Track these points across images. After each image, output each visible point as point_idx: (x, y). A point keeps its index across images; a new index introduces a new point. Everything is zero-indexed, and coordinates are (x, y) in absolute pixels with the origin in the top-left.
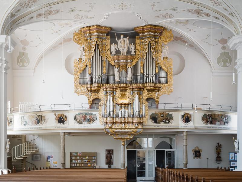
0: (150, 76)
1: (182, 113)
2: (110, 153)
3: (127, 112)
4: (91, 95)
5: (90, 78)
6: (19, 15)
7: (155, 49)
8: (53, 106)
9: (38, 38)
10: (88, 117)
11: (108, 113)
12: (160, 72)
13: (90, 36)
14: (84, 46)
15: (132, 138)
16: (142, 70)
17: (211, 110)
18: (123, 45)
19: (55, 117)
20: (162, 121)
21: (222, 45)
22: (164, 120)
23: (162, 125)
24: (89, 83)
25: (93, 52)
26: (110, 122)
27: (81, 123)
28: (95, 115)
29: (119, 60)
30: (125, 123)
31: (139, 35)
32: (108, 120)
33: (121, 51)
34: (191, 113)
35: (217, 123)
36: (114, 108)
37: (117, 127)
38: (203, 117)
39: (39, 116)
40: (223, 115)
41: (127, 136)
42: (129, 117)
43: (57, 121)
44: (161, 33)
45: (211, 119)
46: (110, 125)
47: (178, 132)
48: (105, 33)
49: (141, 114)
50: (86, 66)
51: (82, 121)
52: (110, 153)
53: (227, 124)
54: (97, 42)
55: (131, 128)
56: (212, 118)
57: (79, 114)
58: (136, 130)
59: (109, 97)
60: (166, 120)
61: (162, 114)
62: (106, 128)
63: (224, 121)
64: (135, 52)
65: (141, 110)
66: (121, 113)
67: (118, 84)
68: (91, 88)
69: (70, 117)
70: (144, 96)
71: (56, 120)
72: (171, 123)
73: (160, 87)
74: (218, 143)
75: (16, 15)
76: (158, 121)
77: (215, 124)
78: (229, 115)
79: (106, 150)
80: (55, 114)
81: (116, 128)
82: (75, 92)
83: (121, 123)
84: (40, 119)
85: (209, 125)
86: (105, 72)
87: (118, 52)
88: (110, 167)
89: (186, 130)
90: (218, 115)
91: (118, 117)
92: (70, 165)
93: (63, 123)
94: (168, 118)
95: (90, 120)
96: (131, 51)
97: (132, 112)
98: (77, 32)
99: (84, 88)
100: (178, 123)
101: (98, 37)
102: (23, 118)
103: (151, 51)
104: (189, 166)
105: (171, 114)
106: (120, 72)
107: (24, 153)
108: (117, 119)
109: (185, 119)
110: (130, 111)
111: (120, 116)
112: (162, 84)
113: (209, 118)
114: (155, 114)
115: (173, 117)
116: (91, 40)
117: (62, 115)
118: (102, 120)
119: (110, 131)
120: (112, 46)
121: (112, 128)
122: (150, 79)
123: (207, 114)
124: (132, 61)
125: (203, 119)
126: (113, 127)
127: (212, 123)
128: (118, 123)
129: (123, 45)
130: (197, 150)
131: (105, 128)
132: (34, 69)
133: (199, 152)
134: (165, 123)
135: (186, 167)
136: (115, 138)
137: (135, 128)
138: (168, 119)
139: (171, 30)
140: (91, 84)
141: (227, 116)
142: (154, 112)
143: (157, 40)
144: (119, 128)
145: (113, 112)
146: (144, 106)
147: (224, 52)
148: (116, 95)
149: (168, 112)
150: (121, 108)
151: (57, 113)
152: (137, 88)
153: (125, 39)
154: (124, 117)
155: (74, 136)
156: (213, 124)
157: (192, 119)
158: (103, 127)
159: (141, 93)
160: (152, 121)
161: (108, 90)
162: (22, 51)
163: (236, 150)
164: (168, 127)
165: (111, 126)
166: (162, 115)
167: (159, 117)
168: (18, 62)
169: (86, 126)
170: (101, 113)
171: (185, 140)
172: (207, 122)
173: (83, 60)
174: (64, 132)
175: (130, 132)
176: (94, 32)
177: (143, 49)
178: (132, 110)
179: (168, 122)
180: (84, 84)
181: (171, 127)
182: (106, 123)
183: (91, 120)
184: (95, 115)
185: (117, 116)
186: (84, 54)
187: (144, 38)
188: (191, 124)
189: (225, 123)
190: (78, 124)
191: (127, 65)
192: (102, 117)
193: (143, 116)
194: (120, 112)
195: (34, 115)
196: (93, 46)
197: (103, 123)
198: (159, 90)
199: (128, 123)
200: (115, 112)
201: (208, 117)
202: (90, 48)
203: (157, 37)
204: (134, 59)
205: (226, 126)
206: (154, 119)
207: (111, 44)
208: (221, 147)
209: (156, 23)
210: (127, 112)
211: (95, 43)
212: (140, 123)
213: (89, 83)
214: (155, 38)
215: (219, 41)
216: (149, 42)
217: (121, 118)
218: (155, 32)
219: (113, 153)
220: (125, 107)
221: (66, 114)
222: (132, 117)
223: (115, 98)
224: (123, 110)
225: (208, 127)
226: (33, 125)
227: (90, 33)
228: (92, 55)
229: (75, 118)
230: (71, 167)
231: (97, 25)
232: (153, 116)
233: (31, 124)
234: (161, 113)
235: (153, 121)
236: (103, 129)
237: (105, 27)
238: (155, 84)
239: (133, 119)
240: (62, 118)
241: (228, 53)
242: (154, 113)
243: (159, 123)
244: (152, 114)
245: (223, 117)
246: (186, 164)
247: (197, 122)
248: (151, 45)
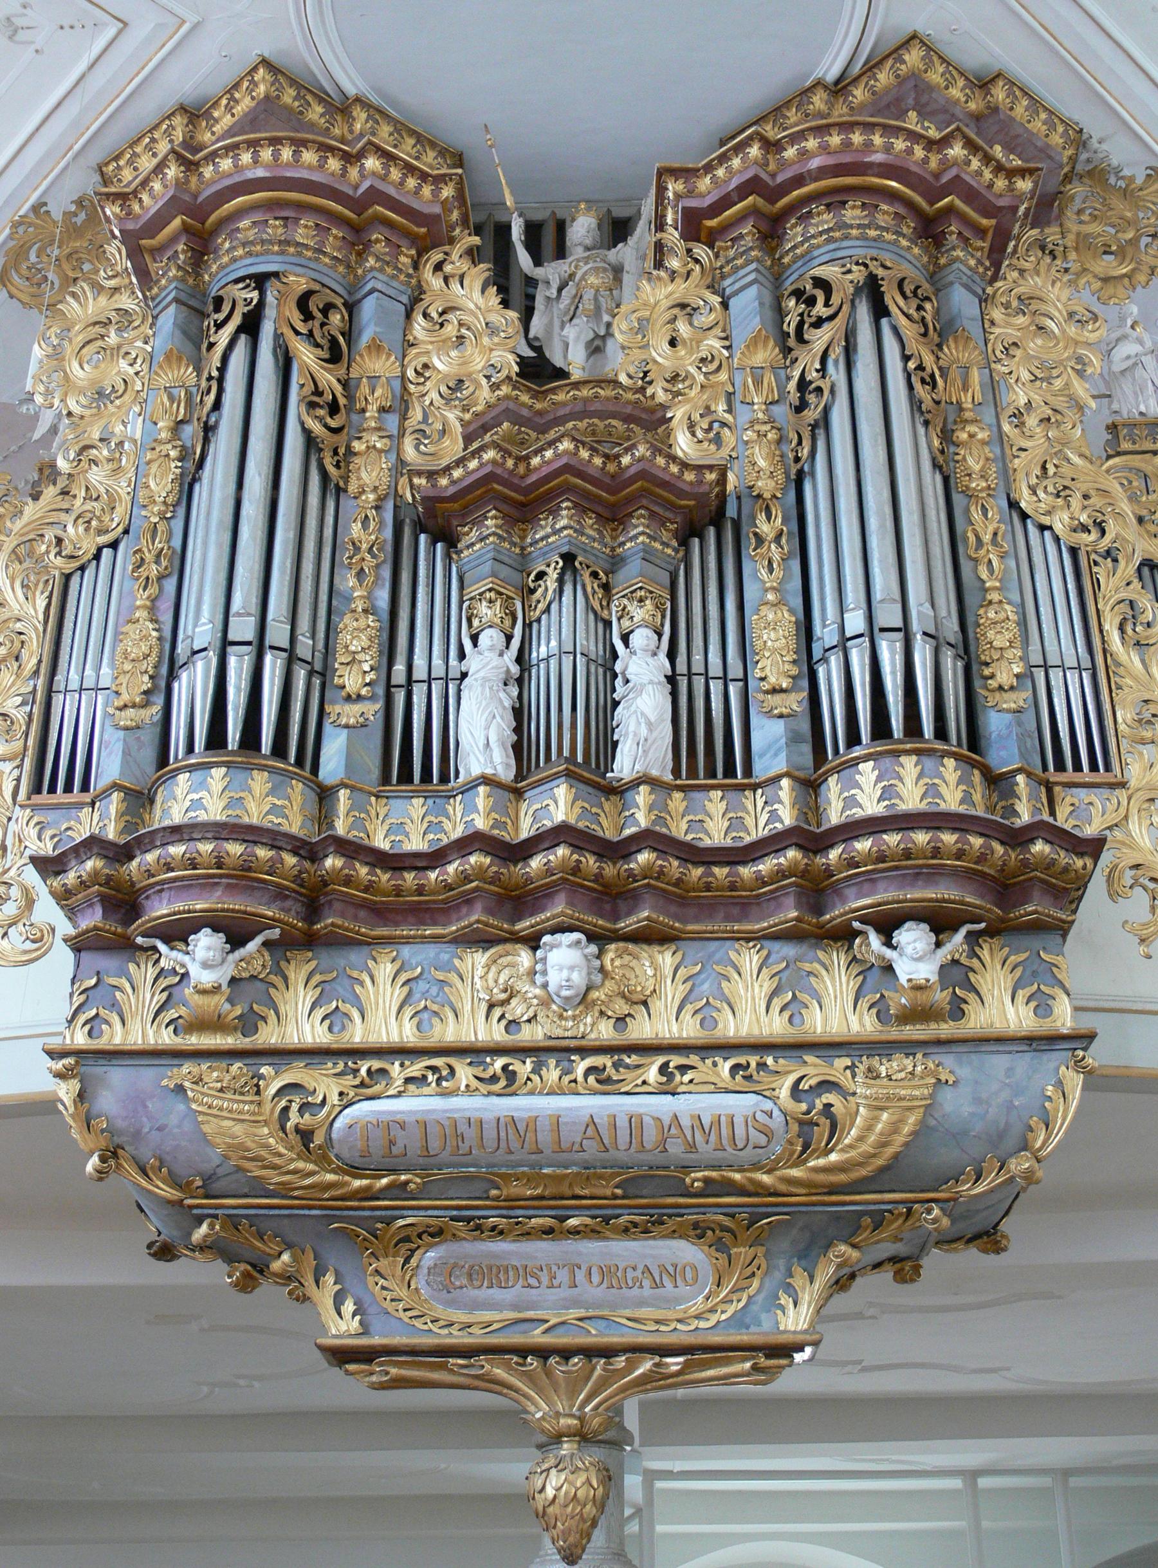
3: (643, 667)
11: (193, 687)
26: (198, 876)
32: (177, 816)
42: (708, 754)
55: (776, 1026)
62: (116, 1036)
81: (357, 1035)
83: (504, 900)
111: (481, 737)
119: (220, 1118)
121: (268, 1036)
126: (299, 1021)
128: (424, 910)
131: (80, 1039)
136: (343, 1327)
137: (862, 1024)
144: (449, 1032)
145: (323, 673)
154: (594, 772)
165: (251, 996)
182: (117, 916)
185: (412, 761)
194: (488, 661)
197: (47, 911)
210: (643, 667)
223: (374, 399)
224: (563, 629)
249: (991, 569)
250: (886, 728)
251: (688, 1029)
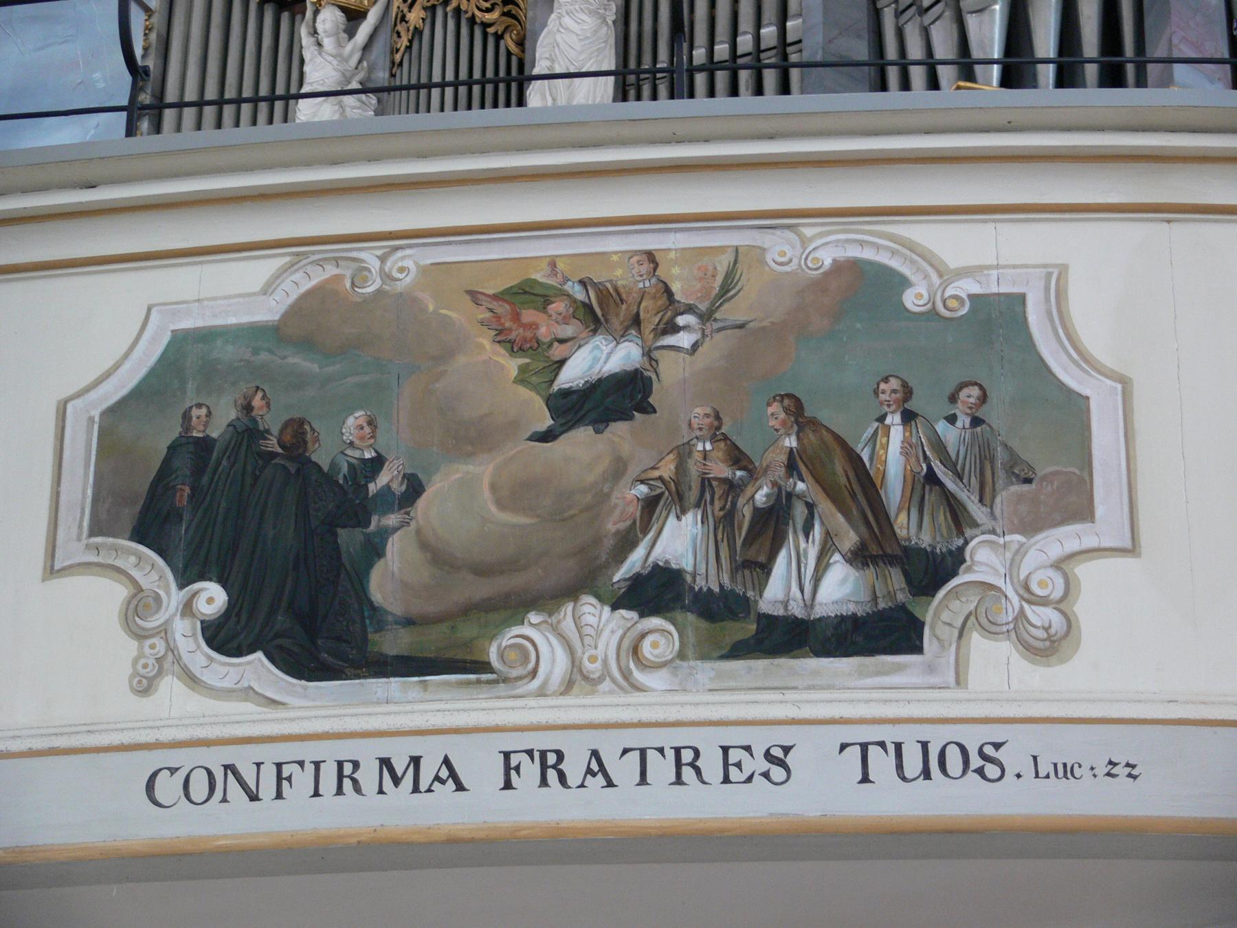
22: (680, 541)
23: (593, 721)
60: (771, 525)
61: (600, 312)
76: (394, 577)
105: (999, 318)
115: (1072, 412)
138: (860, 493)
142: (240, 293)
149: (828, 249)
160: (138, 607)
167: (472, 438)
179: (839, 589)
181: (985, 762)
232: (219, 419)
234: (529, 294)
235: (212, 598)
242: (269, 311)
244: (187, 360)
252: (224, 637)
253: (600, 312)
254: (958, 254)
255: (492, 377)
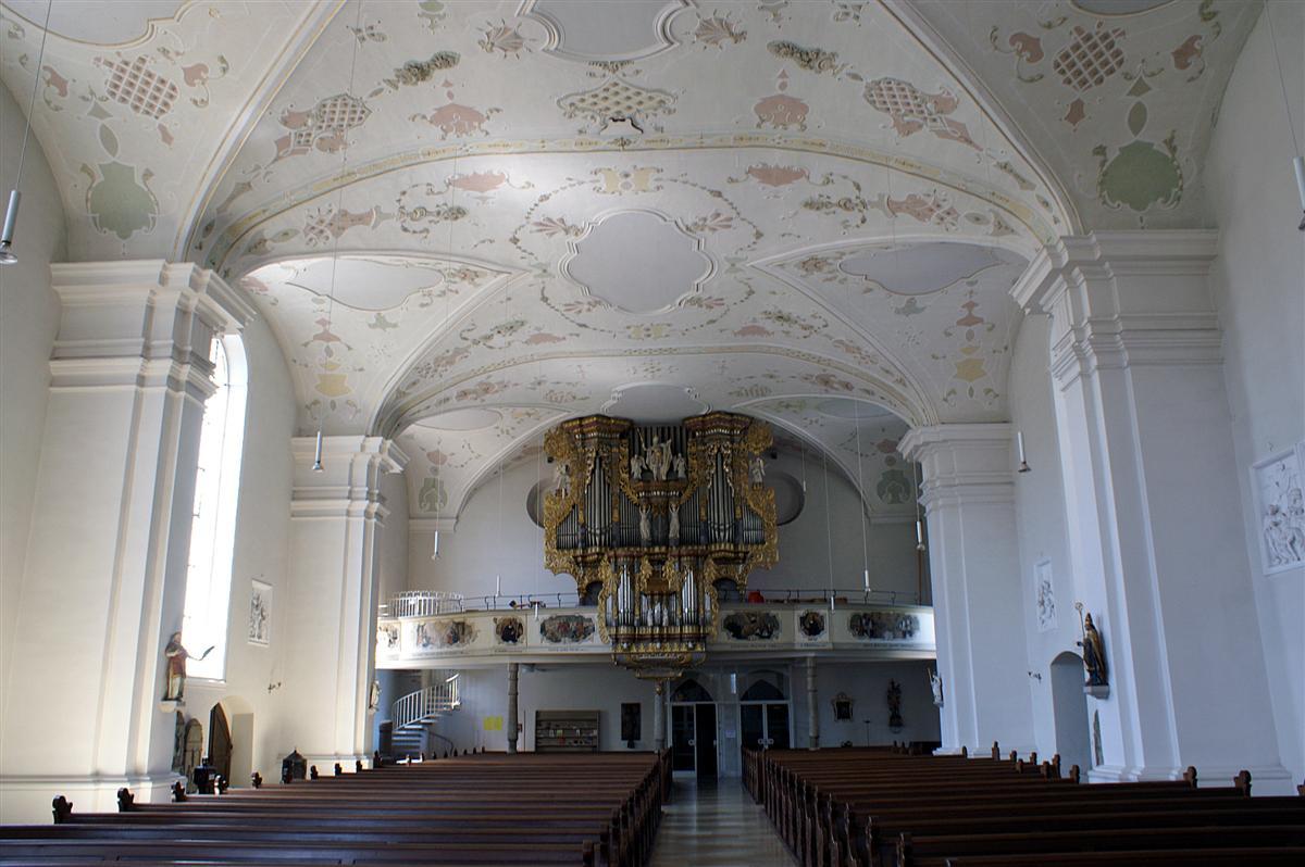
0: (722, 527)
1: (801, 612)
2: (631, 714)
3: (665, 613)
4: (584, 575)
5: (582, 534)
6: (414, 393)
7: (731, 466)
8: (491, 601)
9: (466, 446)
10: (573, 626)
12: (745, 519)
13: (583, 440)
14: (568, 462)
15: (680, 675)
16: (703, 513)
17: (870, 605)
18: (658, 460)
19: (493, 626)
20: (752, 632)
21: (885, 455)
22: (758, 631)
23: (753, 644)
24: (580, 545)
25: (588, 474)
27: (558, 641)
28: (590, 620)
29: (649, 492)
30: (661, 639)
31: (694, 436)
33: (655, 472)
34: (823, 612)
35: (887, 634)
36: (635, 601)
37: (642, 650)
38: (852, 621)
39: (458, 624)
40: (898, 615)
41: (668, 671)
42: (671, 623)
43: (500, 637)
44: (745, 430)
45: (870, 625)
46: (625, 645)
47: (793, 659)
48: (617, 432)
49: (701, 616)
50: (573, 507)
51: (558, 635)
52: (631, 714)
53: (911, 635)
54: (597, 453)
56: (873, 624)
57: (551, 619)
58: (689, 655)
59: (624, 577)
61: (753, 615)
63: (904, 628)
64: (686, 472)
65: (701, 606)
66: (653, 612)
67: (649, 548)
68: (583, 557)
69: (532, 623)
70: (706, 574)
71: (497, 633)
72: (774, 639)
73: (747, 553)
74: (893, 683)
75: (409, 394)
77: (881, 637)
78: (912, 614)
79: (623, 705)
80: (495, 620)
82: (548, 566)
83: (653, 639)
84: (458, 633)
85: (866, 640)
86: (615, 520)
87: (646, 471)
88: (631, 745)
89: (813, 655)
90: (889, 614)
91: (646, 625)
92: (536, 742)
93: (515, 641)
94: (768, 627)
95: (578, 634)
96: (677, 471)
97: (678, 613)
98: (553, 431)
99: (564, 559)
100: (791, 635)
101: (601, 441)
102: (420, 628)
103: (723, 470)
104: (824, 743)
106: (651, 521)
107: (423, 714)
108: (643, 631)
109: (808, 626)
110: (673, 609)
111: (650, 623)
112: (752, 544)
113: (867, 624)
114: (736, 615)
116: (584, 448)
117: (512, 621)
118: (607, 634)
119: (626, 658)
120: (633, 462)
122: (722, 534)
123: (861, 612)
124: (680, 494)
125: (852, 627)
127: (873, 635)
129: (658, 460)
130: (843, 700)
132: (457, 518)
133: (847, 704)
134: (762, 637)
135: (817, 745)
139: (767, 422)
140: (585, 548)
141: (909, 617)
142: (732, 612)
143: (736, 445)
146: (707, 597)
147: (893, 471)
148: (639, 571)
150: (652, 604)
151: (499, 618)
152: (690, 556)
153: (662, 445)
154: (661, 626)
155: (544, 670)
156: (876, 637)
157: (826, 626)
158: (609, 650)
159: (700, 566)
161: (621, 560)
162: (432, 476)
163: (937, 700)
164: (767, 648)
165: (629, 648)
166: (753, 619)
168: (421, 501)
169: (568, 647)
170: (603, 615)
171: (809, 679)
172: (862, 632)
173: (566, 494)
174: (517, 664)
175: (673, 661)
176: (592, 431)
177: (704, 466)
178: (679, 608)
180: (569, 549)
182: (616, 640)
183: (581, 631)
184: (590, 620)
185: (643, 623)
186: (568, 479)
187: (706, 441)
188: (823, 638)
189: (904, 636)
190: (548, 644)
191: (668, 502)
192: (607, 625)
193: (706, 623)
194: (650, 612)
195: (446, 621)
196: (589, 462)
198: (744, 559)
199: (670, 638)
200: (637, 612)
201: (864, 621)
202: (582, 465)
203: (737, 439)
204: (685, 489)
205: (908, 641)
206: (734, 627)
207: (631, 456)
208: (900, 692)
209: (734, 407)
210: (665, 613)
211: (594, 454)
212: (698, 638)
213: (580, 545)
214: (732, 442)
215: (879, 446)
216: (719, 450)
217: (652, 627)
218: (732, 430)
219: (639, 712)
220: (661, 601)
221: (521, 618)
222: (678, 624)
223: (637, 579)
224: (657, 608)
225: (866, 645)
226: (442, 646)
227: (583, 434)
228: (588, 482)
229: (543, 629)
230: (537, 747)
231: (597, 416)
233: (438, 643)
236: (609, 655)
237: (616, 419)
238: (736, 546)
239: (681, 630)
240: (511, 630)
241: (902, 472)
243: (745, 638)
244: (729, 617)
245: (900, 619)
246: (817, 738)
247: (837, 631)
248: (722, 458)
249: (701, 601)
250: (689, 623)
251: (669, 650)
252: (733, 636)
253: (753, 615)
254: (773, 612)
255: (747, 619)
